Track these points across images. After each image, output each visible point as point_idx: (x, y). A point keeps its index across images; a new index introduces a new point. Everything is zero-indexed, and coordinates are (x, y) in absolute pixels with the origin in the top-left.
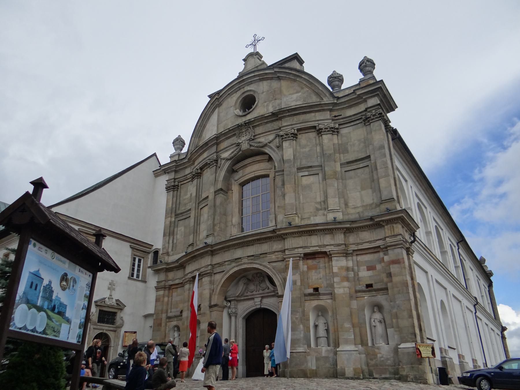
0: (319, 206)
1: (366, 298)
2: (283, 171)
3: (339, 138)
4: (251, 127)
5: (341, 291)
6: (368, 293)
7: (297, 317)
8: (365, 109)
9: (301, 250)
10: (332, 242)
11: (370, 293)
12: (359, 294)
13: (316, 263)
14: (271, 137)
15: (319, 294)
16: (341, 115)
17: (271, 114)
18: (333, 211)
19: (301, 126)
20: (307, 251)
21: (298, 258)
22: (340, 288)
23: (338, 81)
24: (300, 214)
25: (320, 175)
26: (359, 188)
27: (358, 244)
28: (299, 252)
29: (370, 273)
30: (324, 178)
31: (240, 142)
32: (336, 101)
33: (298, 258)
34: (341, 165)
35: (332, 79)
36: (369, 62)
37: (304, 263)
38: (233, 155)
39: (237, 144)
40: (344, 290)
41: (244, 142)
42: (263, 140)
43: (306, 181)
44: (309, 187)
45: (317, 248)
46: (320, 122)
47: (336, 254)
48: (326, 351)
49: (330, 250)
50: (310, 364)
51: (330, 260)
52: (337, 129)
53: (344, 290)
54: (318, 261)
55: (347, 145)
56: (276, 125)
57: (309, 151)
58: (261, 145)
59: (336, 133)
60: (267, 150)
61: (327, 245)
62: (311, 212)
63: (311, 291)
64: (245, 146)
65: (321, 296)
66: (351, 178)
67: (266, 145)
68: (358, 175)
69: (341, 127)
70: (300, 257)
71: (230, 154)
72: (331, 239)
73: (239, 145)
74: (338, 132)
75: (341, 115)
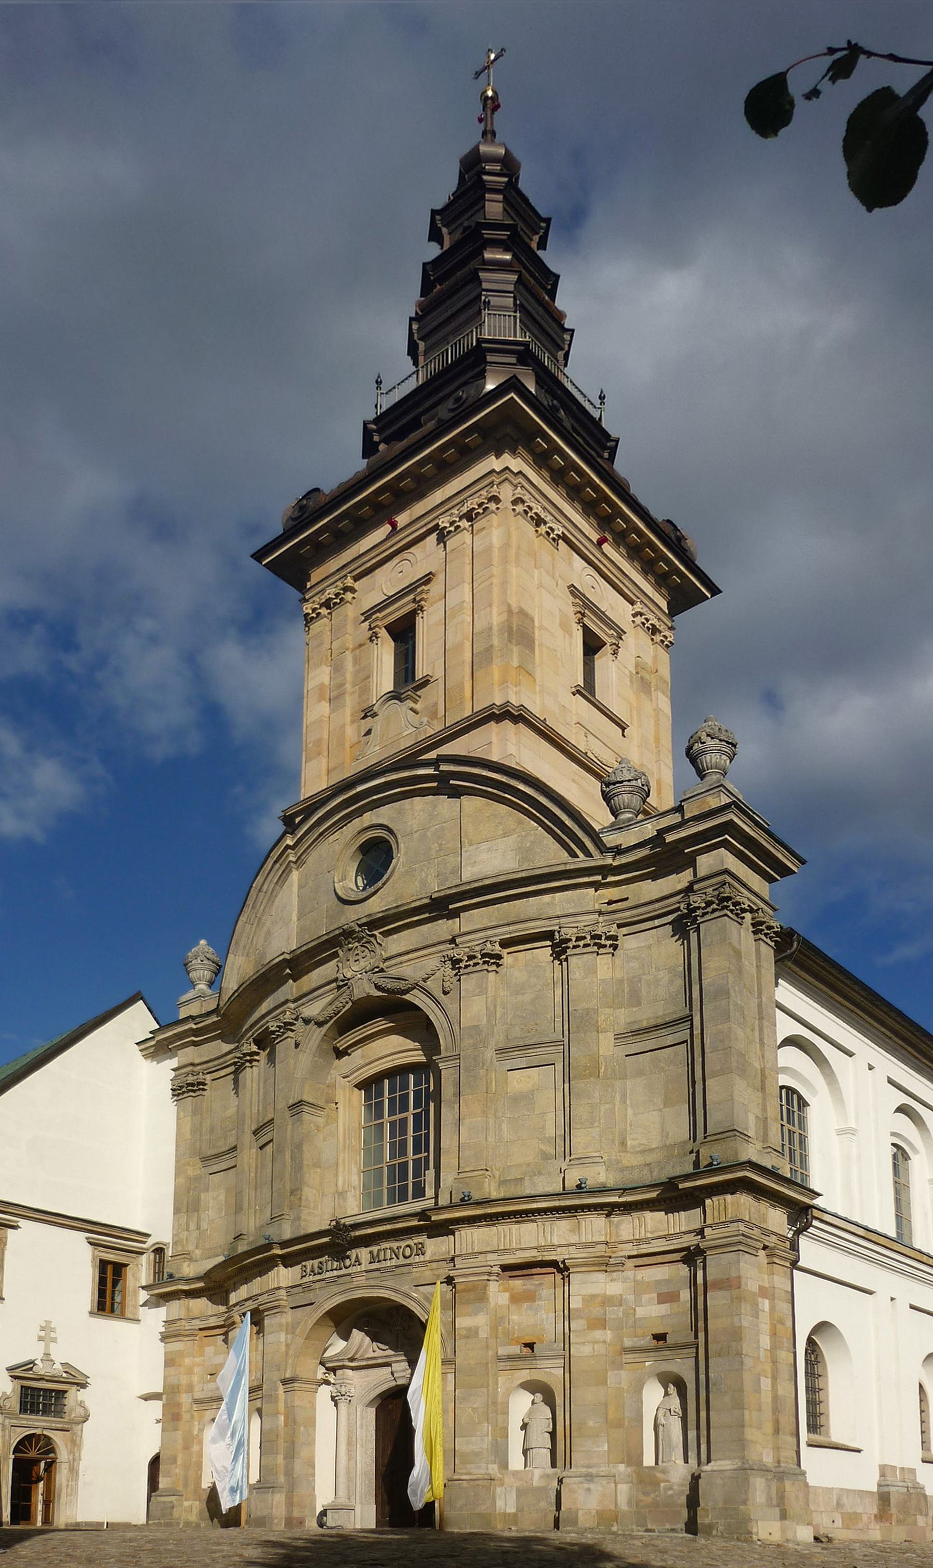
0: (550, 1150)
1: (647, 1364)
2: (458, 1057)
3: (618, 961)
4: (378, 935)
5: (587, 1350)
6: (652, 1354)
7: (475, 1406)
8: (687, 884)
9: (495, 1256)
10: (574, 1239)
11: (657, 1354)
12: (630, 1357)
13: (533, 1287)
14: (431, 962)
15: (535, 1358)
16: (627, 899)
17: (427, 901)
18: (582, 1161)
19: (510, 933)
20: (510, 1259)
21: (486, 1277)
22: (584, 1343)
23: (630, 792)
24: (497, 1170)
25: (559, 1066)
26: (659, 1101)
27: (639, 1241)
28: (489, 1263)
29: (664, 1309)
30: (567, 1077)
31: (349, 976)
32: (609, 861)
33: (486, 1277)
34: (615, 1039)
35: (612, 787)
36: (712, 738)
37: (501, 1288)
38: (330, 1011)
39: (342, 981)
40: (593, 1348)
41: (359, 976)
42: (410, 970)
43: (520, 1081)
44: (525, 1099)
45: (534, 1253)
46: (563, 920)
47: (582, 1265)
48: (541, 1477)
49: (567, 1257)
50: (500, 1504)
51: (566, 1279)
52: (615, 938)
53: (593, 1348)
54: (537, 1282)
55: (640, 981)
56: (443, 928)
57: (533, 1000)
58: (402, 985)
59: (611, 950)
60: (418, 998)
61: (560, 1246)
62: (528, 1164)
63: (516, 1349)
64: (364, 988)
65: (538, 1362)
66: (640, 1073)
67: (416, 986)
68: (662, 1065)
69: (625, 930)
70: (490, 1274)
71: (323, 1010)
72: (572, 1231)
73: (346, 984)
74: (615, 947)
75: (627, 899)
